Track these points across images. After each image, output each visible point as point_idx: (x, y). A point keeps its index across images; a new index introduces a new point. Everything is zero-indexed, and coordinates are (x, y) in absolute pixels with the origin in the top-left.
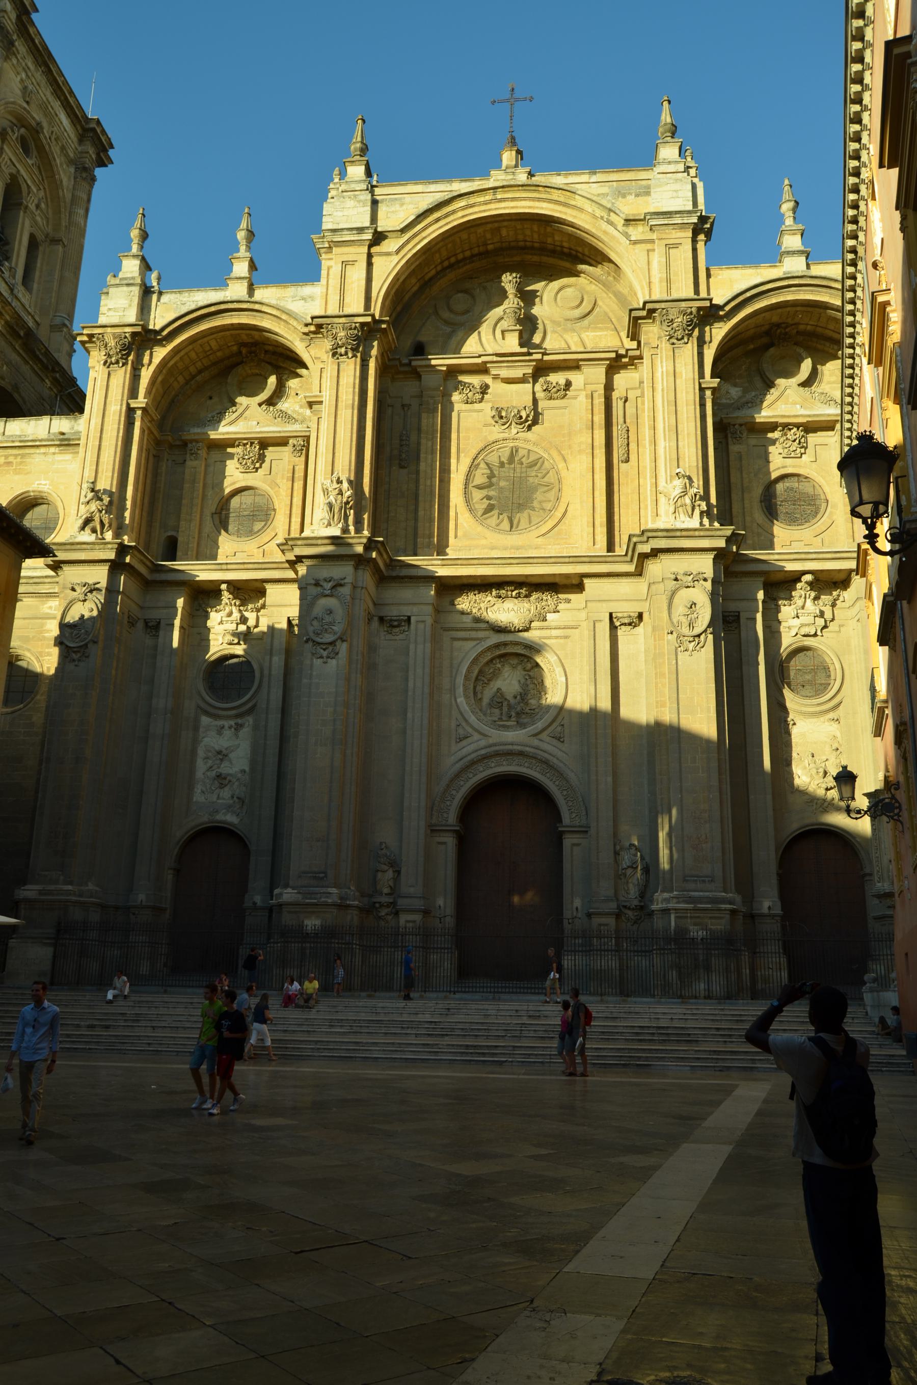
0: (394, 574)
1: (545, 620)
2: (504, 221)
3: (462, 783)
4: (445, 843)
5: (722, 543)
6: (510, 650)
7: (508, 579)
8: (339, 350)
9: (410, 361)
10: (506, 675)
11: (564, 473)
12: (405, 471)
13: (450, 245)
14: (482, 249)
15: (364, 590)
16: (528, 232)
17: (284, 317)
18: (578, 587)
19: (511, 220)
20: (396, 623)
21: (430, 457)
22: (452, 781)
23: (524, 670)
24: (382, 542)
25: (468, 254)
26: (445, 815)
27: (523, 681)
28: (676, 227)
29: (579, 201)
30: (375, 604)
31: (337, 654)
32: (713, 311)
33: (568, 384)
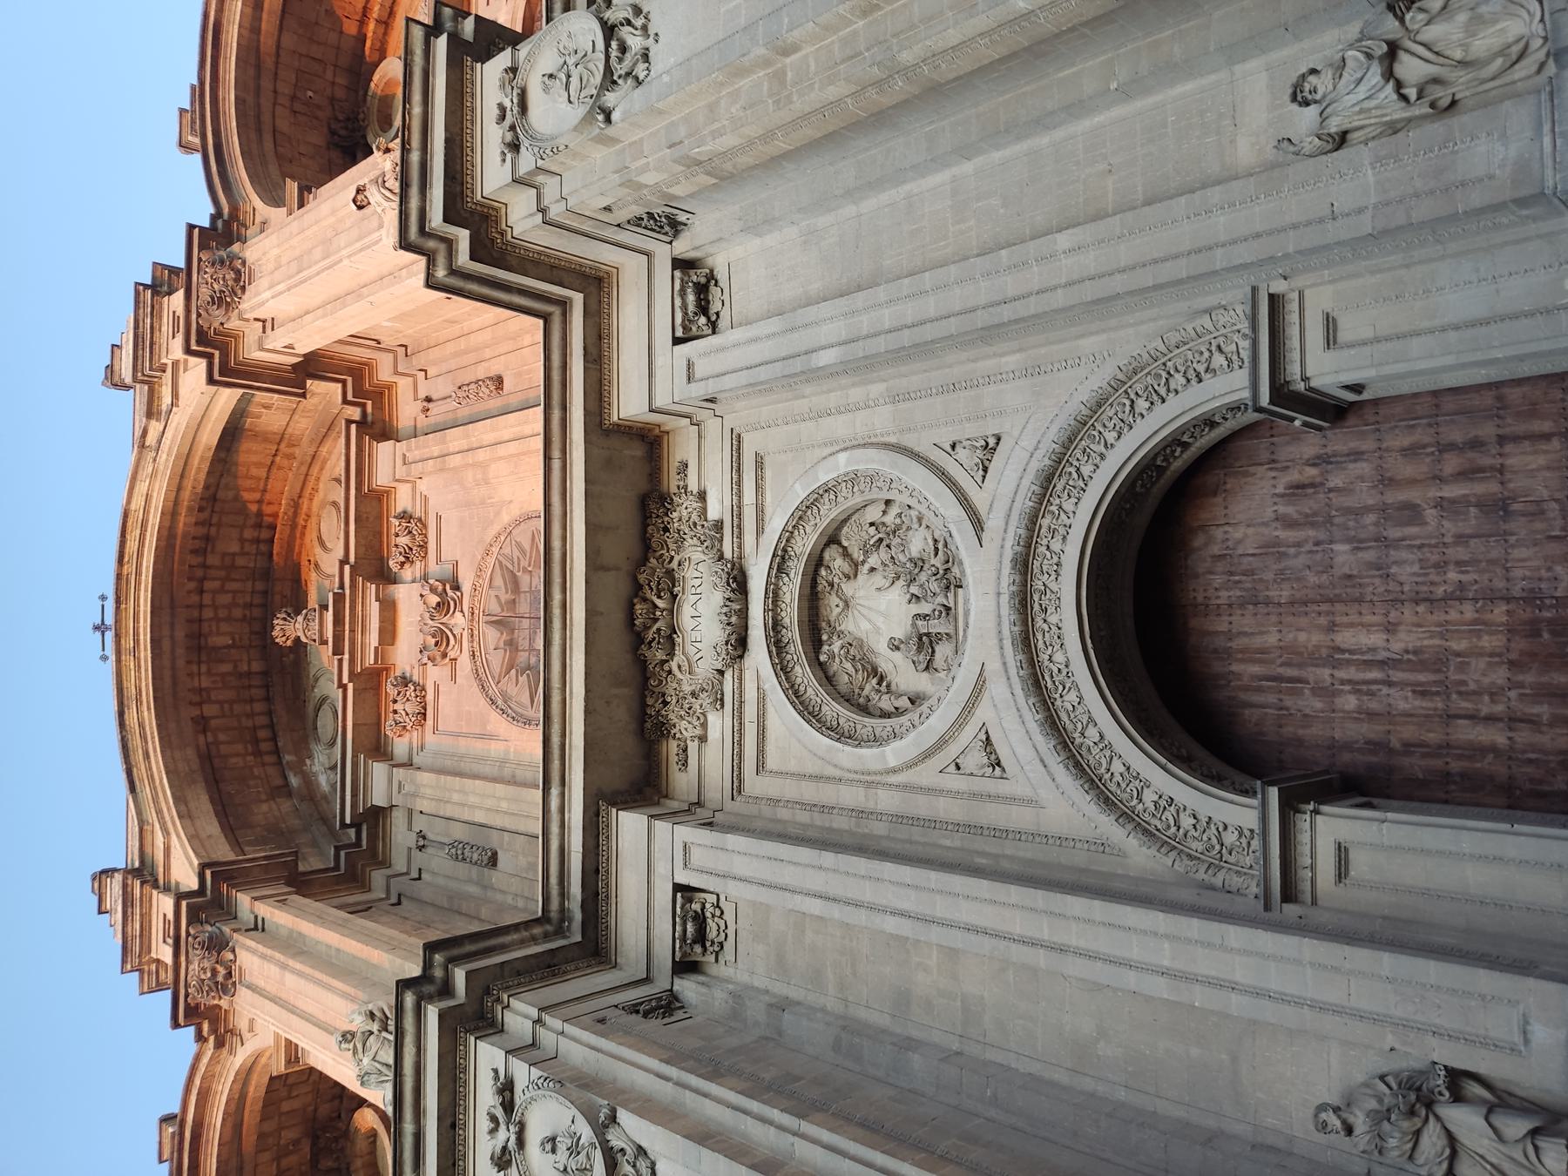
0: (578, 916)
1: (719, 526)
2: (172, 637)
3: (1117, 767)
4: (1342, 852)
5: (441, 43)
6: (791, 613)
7: (617, 617)
8: (220, 979)
9: (343, 825)
10: (865, 625)
11: (515, 511)
12: (502, 858)
13: (222, 737)
14: (256, 681)
15: (547, 1018)
16: (225, 599)
17: (197, 1082)
18: (648, 442)
19: (172, 625)
20: (690, 928)
21: (472, 799)
22: (1107, 801)
23: (851, 576)
24: (431, 948)
25: (259, 707)
26: (1230, 838)
27: (879, 580)
28: (156, 325)
29: (138, 502)
30: (647, 980)
31: (641, 1151)
32: (220, 224)
33: (405, 516)
